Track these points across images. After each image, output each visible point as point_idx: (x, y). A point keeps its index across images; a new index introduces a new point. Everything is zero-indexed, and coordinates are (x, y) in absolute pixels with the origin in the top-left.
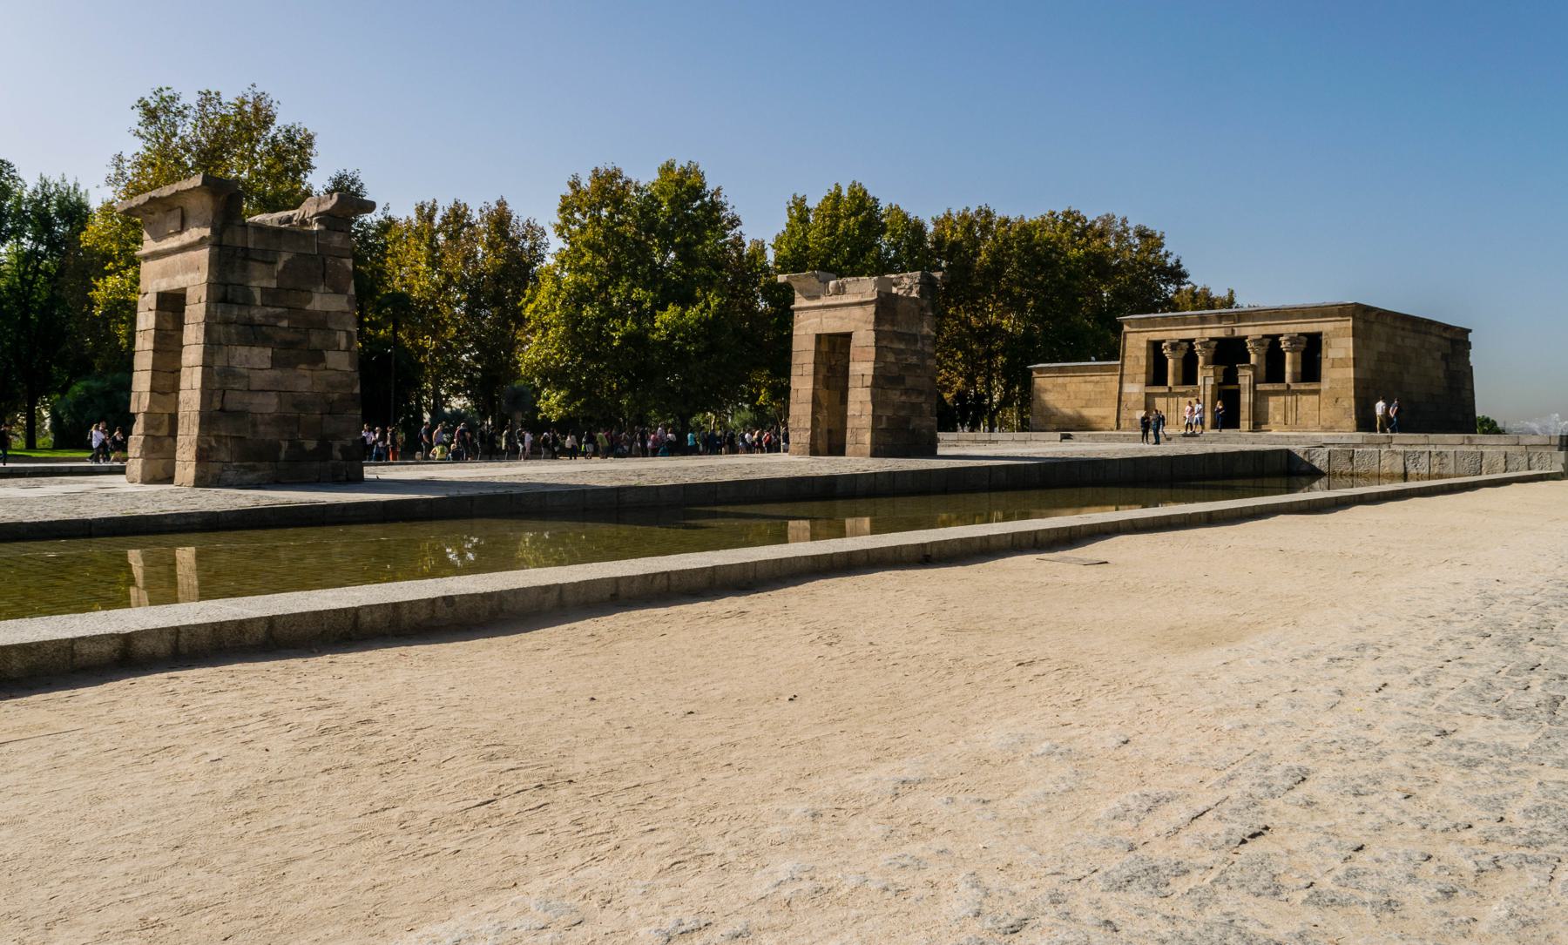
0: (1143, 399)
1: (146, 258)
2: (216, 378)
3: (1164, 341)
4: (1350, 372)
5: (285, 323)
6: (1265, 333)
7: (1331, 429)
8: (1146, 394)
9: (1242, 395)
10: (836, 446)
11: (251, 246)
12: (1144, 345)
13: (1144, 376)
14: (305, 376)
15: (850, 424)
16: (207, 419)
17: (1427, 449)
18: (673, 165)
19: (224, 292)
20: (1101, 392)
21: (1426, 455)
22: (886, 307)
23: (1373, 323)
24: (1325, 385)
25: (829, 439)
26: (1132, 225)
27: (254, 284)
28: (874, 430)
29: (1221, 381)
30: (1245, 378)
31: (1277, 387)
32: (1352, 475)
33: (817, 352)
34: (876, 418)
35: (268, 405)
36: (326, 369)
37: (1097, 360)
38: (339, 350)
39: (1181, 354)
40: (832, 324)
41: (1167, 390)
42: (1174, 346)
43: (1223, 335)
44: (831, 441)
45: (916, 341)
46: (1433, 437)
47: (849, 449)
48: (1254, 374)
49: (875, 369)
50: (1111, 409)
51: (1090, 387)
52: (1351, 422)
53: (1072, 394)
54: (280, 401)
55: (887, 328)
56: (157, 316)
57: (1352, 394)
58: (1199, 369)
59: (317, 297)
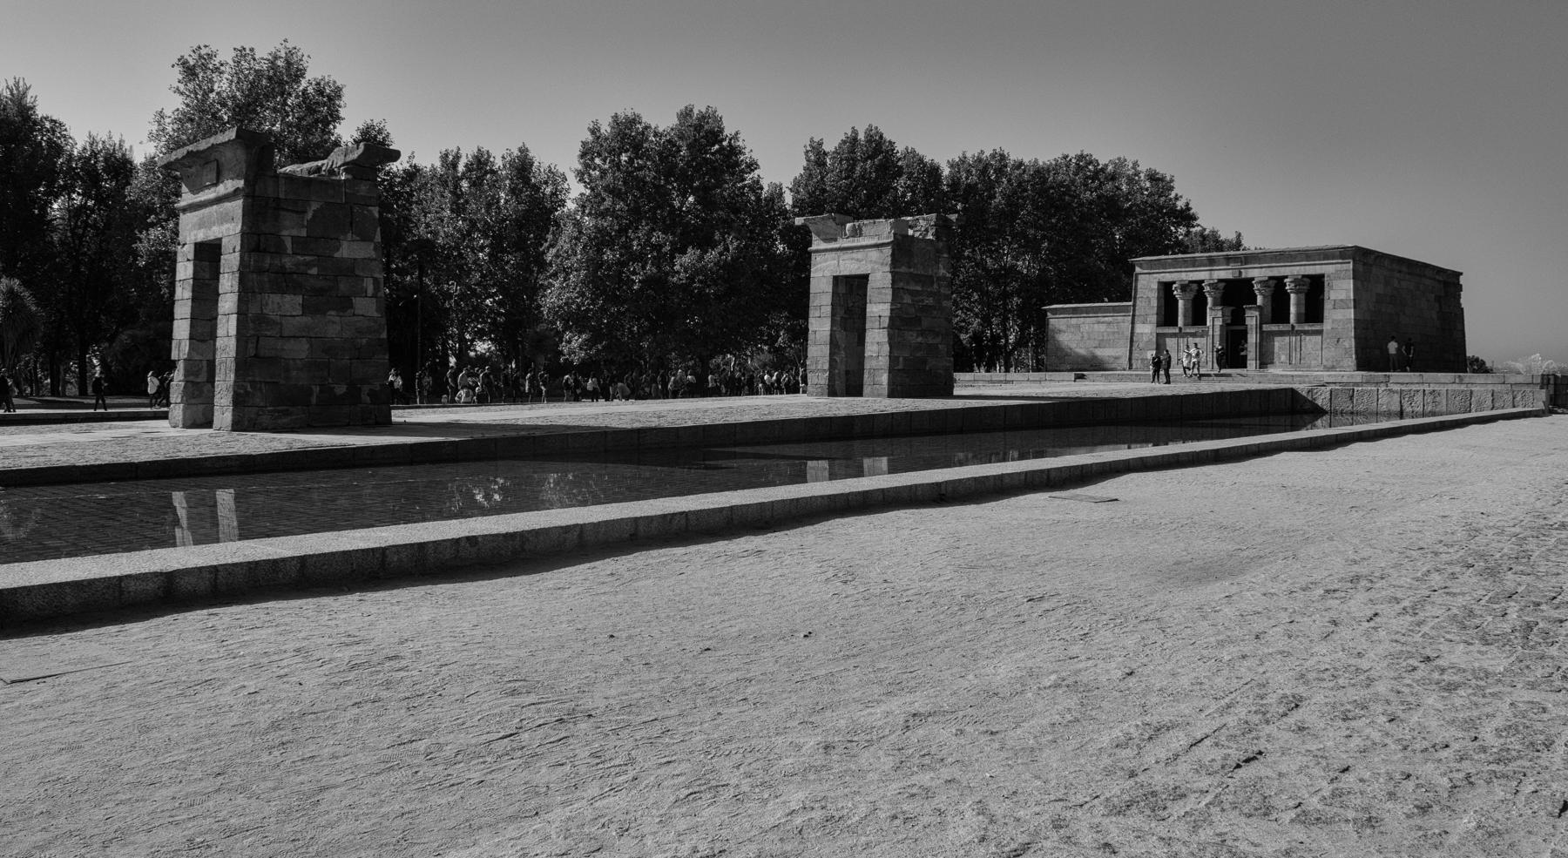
0: (1154, 339)
1: (185, 210)
2: (251, 325)
3: (1174, 283)
4: (1351, 314)
5: (314, 271)
6: (1271, 274)
7: (1333, 368)
8: (1157, 334)
9: (1249, 336)
10: (853, 387)
11: (282, 196)
12: (1155, 286)
13: (1155, 316)
14: (334, 323)
15: (867, 365)
16: (243, 364)
17: (1421, 388)
18: (691, 110)
19: (256, 240)
20: (1114, 333)
21: (1421, 393)
22: (902, 249)
23: (1371, 265)
24: (1327, 326)
25: (847, 380)
26: (1143, 168)
27: (285, 233)
28: (891, 370)
29: (1229, 322)
30: (1252, 319)
31: (1282, 327)
32: (1352, 413)
33: (834, 293)
34: (893, 359)
35: (299, 350)
36: (354, 315)
37: (1109, 301)
39: (1191, 296)
40: (849, 266)
41: (1177, 331)
42: (1184, 288)
43: (1230, 277)
44: (848, 381)
45: (932, 283)
46: (1428, 376)
47: (867, 389)
48: (1260, 315)
49: (892, 310)
51: (1103, 327)
52: (1351, 361)
53: (1085, 335)
54: (311, 346)
55: (903, 269)
56: (195, 266)
57: (1353, 334)
59: (345, 244)
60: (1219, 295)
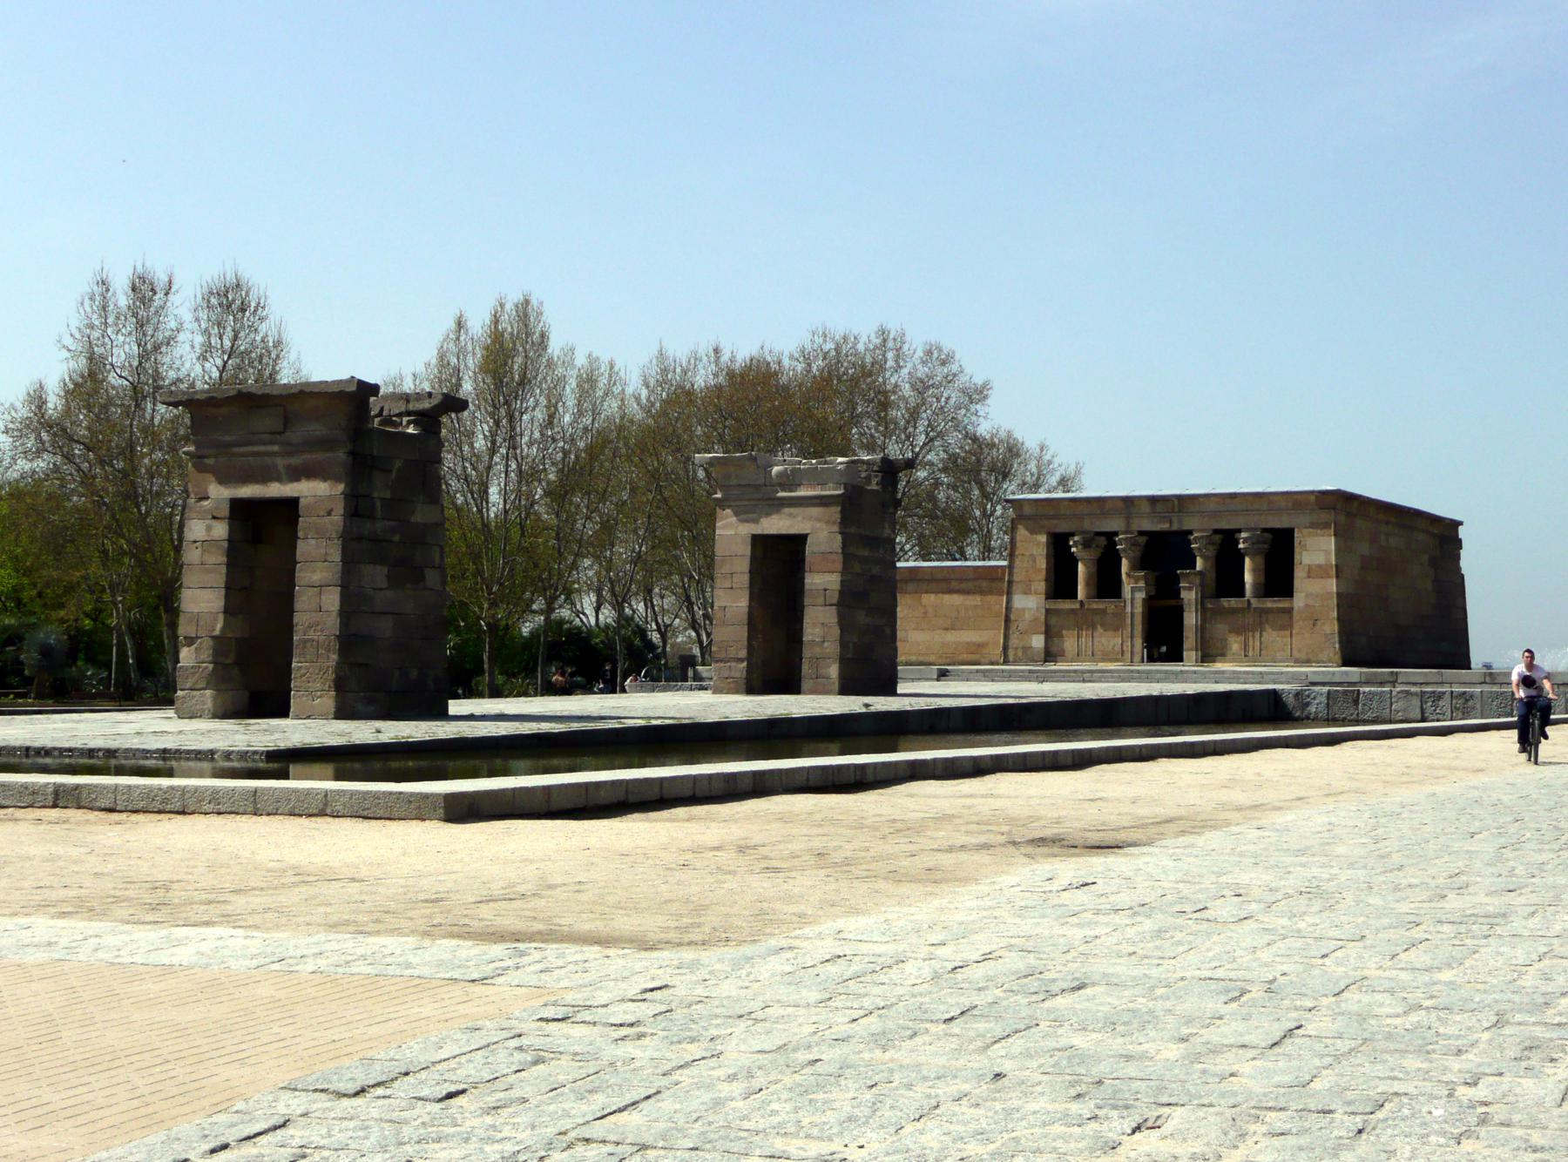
0: (1043, 618)
3: (1073, 534)
4: (1332, 585)
5: (396, 538)
8: (1048, 611)
9: (1185, 614)
13: (1043, 584)
15: (807, 653)
21: (1447, 696)
24: (1299, 601)
27: (375, 495)
29: (1153, 594)
34: (843, 644)
38: (434, 567)
39: (1094, 554)
41: (1077, 606)
47: (805, 685)
50: (992, 633)
53: (930, 610)
55: (853, 530)
57: (1335, 614)
58: (1124, 576)
60: (1138, 554)
